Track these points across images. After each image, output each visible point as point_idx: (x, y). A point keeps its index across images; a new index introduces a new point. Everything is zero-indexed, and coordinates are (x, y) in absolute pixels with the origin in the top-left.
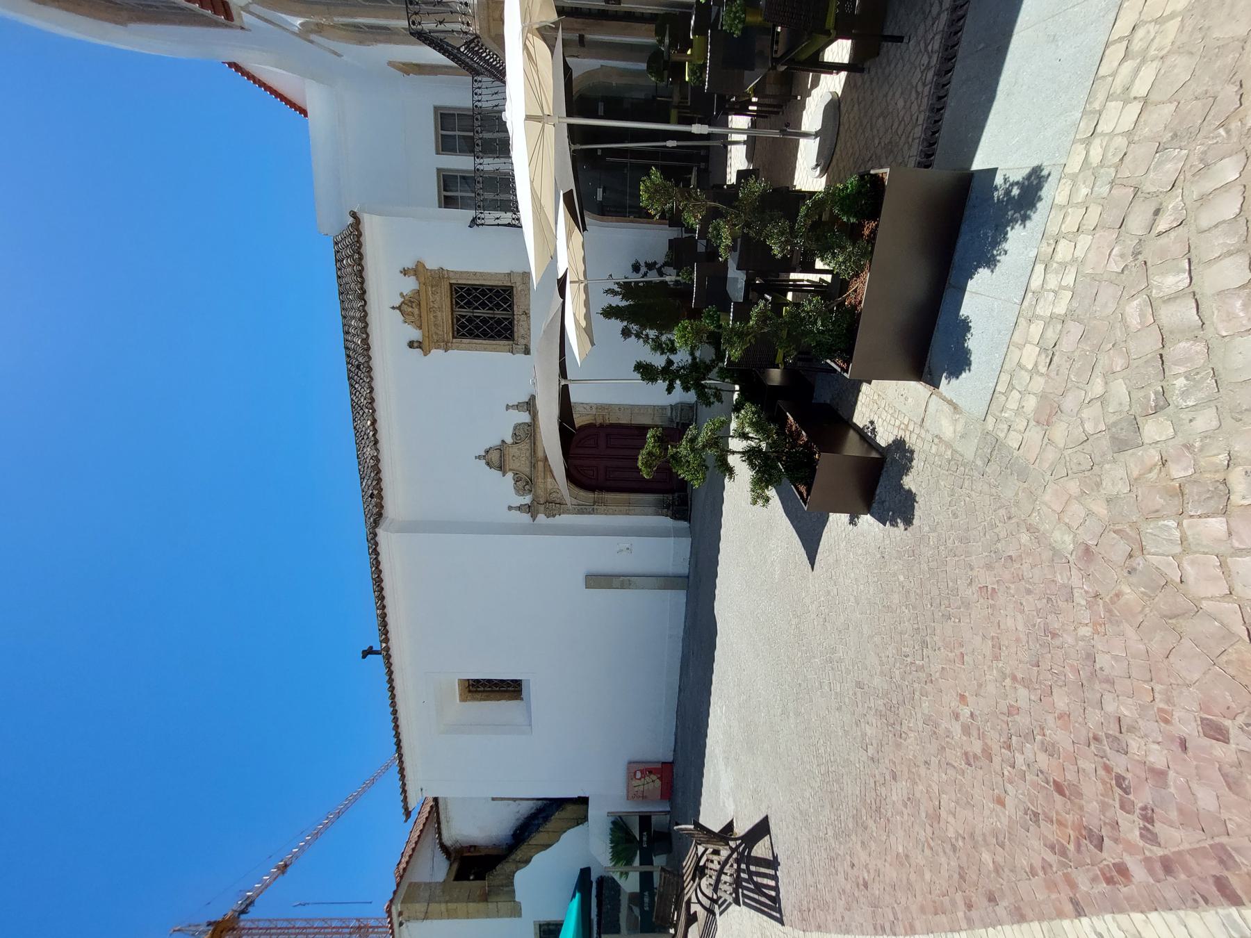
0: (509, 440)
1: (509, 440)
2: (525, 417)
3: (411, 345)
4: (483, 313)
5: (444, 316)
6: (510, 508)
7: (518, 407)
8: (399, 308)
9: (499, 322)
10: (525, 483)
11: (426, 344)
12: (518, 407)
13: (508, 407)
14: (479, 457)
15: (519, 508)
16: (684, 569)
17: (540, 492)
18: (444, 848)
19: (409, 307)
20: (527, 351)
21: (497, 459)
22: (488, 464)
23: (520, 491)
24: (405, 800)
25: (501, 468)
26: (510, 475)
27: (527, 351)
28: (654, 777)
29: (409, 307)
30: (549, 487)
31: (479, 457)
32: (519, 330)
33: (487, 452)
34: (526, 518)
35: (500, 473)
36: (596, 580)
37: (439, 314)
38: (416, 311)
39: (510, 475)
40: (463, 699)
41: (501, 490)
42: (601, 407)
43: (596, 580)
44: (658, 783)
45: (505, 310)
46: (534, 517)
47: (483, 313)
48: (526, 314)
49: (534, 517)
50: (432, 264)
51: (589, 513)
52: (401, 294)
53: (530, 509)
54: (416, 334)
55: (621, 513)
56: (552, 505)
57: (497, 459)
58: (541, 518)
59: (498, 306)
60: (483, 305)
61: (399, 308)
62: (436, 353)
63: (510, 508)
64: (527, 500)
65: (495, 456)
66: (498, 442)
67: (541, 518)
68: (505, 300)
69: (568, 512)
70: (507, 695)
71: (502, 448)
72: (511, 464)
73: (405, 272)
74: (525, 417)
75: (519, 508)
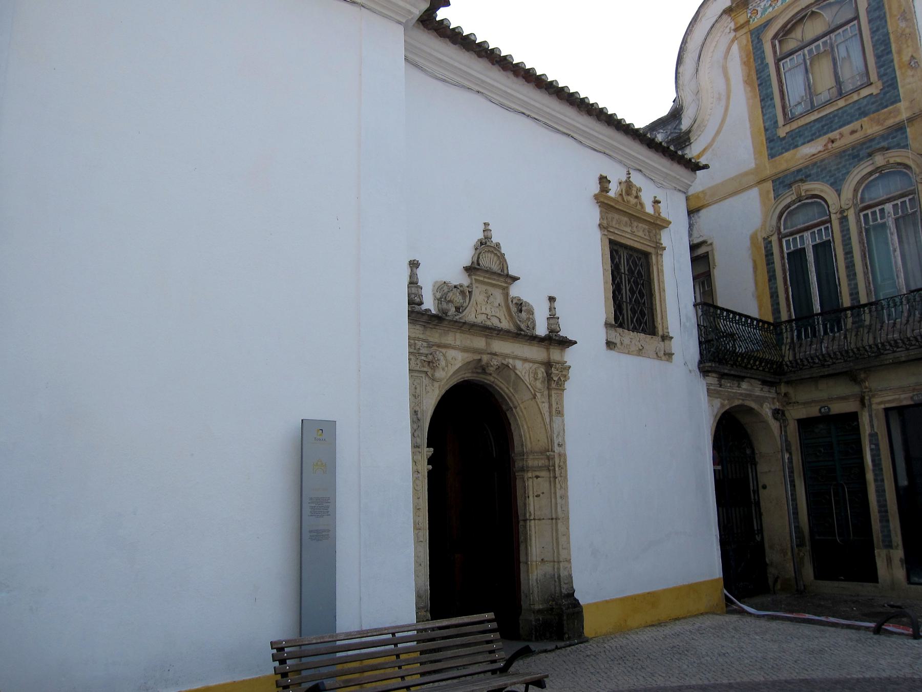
0: (515, 291)
1: (515, 291)
3: (603, 181)
6: (414, 265)
7: (552, 317)
12: (552, 317)
13: (552, 299)
15: (413, 282)
23: (444, 291)
27: (610, 345)
30: (451, 353)
36: (313, 451)
42: (553, 465)
43: (313, 451)
63: (414, 265)
64: (429, 304)
66: (512, 272)
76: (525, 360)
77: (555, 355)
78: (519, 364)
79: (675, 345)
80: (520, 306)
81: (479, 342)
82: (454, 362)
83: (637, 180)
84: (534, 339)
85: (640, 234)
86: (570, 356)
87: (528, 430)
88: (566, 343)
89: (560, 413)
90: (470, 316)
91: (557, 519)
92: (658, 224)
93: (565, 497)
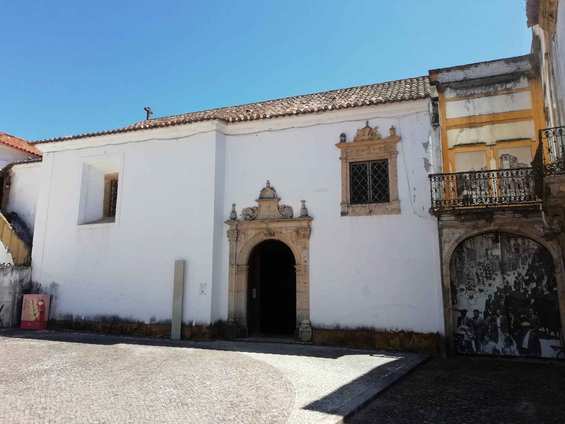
1: (281, 203)
3: (343, 135)
4: (370, 182)
5: (364, 156)
6: (234, 205)
7: (304, 208)
8: (367, 126)
9: (365, 193)
10: (251, 216)
11: (344, 145)
12: (304, 208)
13: (303, 202)
14: (268, 183)
15: (234, 212)
18: (10, 167)
19: (369, 134)
20: (343, 214)
21: (268, 195)
22: (264, 189)
24: (41, 142)
25: (261, 198)
26: (256, 205)
27: (343, 214)
28: (38, 315)
29: (369, 134)
31: (268, 183)
32: (358, 207)
33: (272, 189)
34: (227, 215)
35: (257, 197)
36: (181, 268)
37: (365, 152)
38: (366, 137)
39: (256, 205)
41: (246, 199)
42: (306, 270)
43: (181, 268)
44: (33, 318)
45: (373, 197)
46: (227, 222)
47: (370, 182)
49: (227, 222)
50: (399, 146)
51: (230, 262)
52: (377, 128)
53: (234, 219)
54: (350, 138)
55: (230, 285)
56: (236, 234)
57: (268, 195)
58: (227, 227)
59: (375, 192)
60: (375, 182)
61: (367, 126)
62: (338, 152)
63: (234, 205)
64: (239, 217)
65: (269, 194)
67: (227, 227)
68: (380, 197)
69: (231, 248)
70: (108, 206)
71: (275, 198)
72: (265, 204)
73: (393, 129)
75: (234, 212)
76: (286, 228)
78: (284, 231)
79: (405, 204)
81: (264, 226)
82: (253, 236)
83: (372, 125)
84: (297, 220)
85: (377, 151)
86: (314, 224)
90: (261, 215)
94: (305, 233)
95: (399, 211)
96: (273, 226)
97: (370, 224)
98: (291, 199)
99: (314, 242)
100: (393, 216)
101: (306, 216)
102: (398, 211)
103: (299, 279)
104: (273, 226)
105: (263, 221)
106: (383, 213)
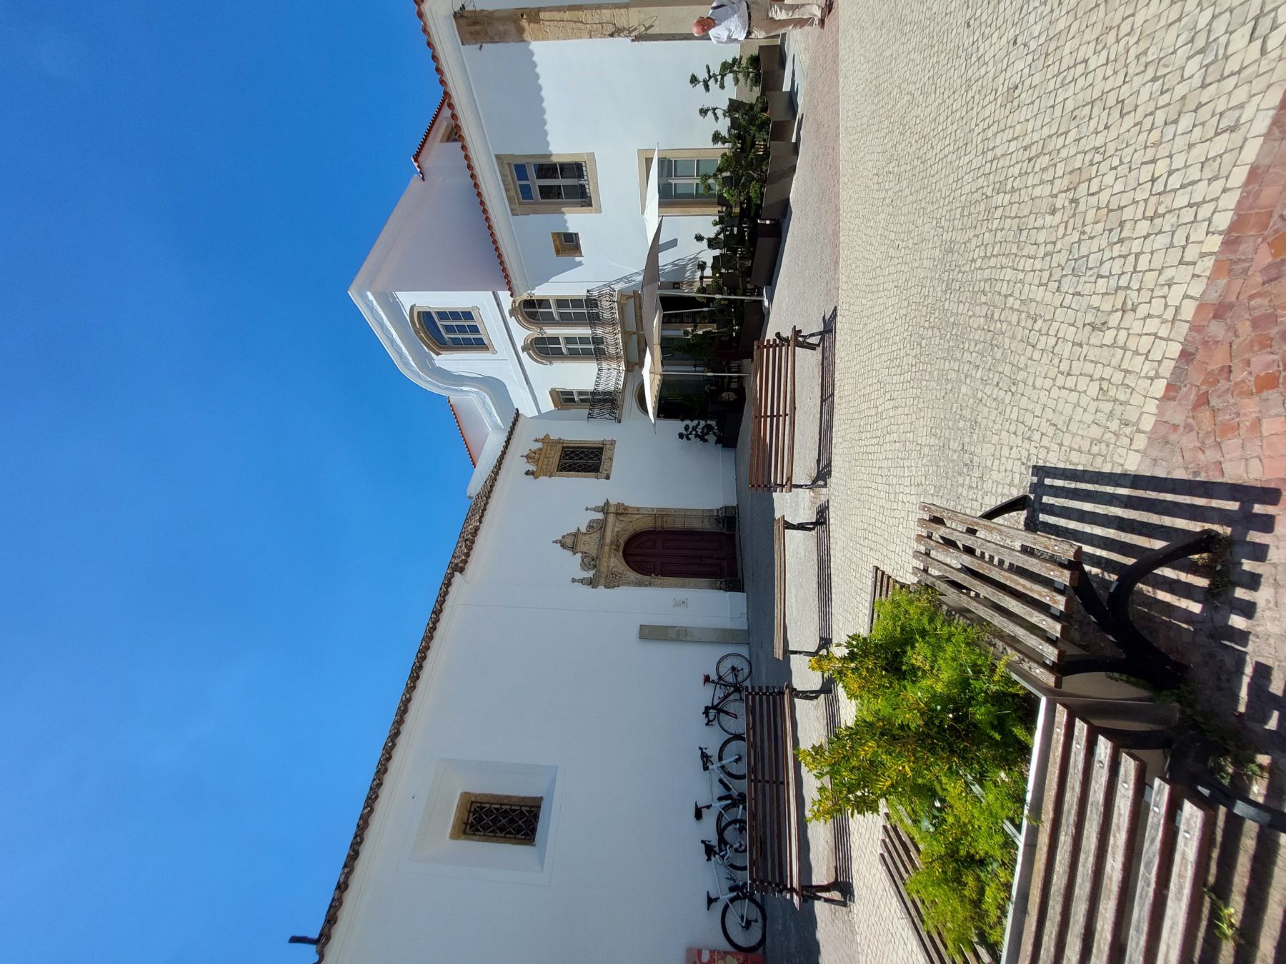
0: (583, 530)
1: (583, 530)
2: (600, 516)
3: (527, 473)
6: (574, 580)
7: (594, 509)
10: (591, 562)
12: (594, 509)
15: (582, 581)
16: (742, 624)
17: (603, 569)
20: (608, 477)
21: (570, 543)
23: (585, 566)
25: (573, 549)
26: (579, 555)
27: (608, 477)
32: (604, 466)
36: (650, 633)
39: (579, 555)
40: (454, 836)
41: (572, 564)
42: (662, 514)
43: (650, 633)
48: (611, 459)
54: (532, 468)
56: (612, 581)
57: (570, 543)
63: (574, 580)
64: (590, 574)
65: (569, 542)
71: (576, 535)
72: (581, 547)
74: (600, 516)
75: (582, 581)
77: (612, 509)
80: (590, 527)
81: (607, 548)
82: (616, 562)
86: (613, 502)
87: (645, 524)
88: (607, 503)
89: (638, 509)
91: (686, 514)
92: (546, 440)
93: (676, 510)
94: (622, 511)
95: (613, 442)
96: (608, 540)
97: (619, 463)
98: (581, 521)
99: (632, 501)
100: (617, 445)
101: (605, 509)
102: (613, 442)
103: (669, 524)
104: (608, 540)
105: (602, 545)
106: (613, 450)
